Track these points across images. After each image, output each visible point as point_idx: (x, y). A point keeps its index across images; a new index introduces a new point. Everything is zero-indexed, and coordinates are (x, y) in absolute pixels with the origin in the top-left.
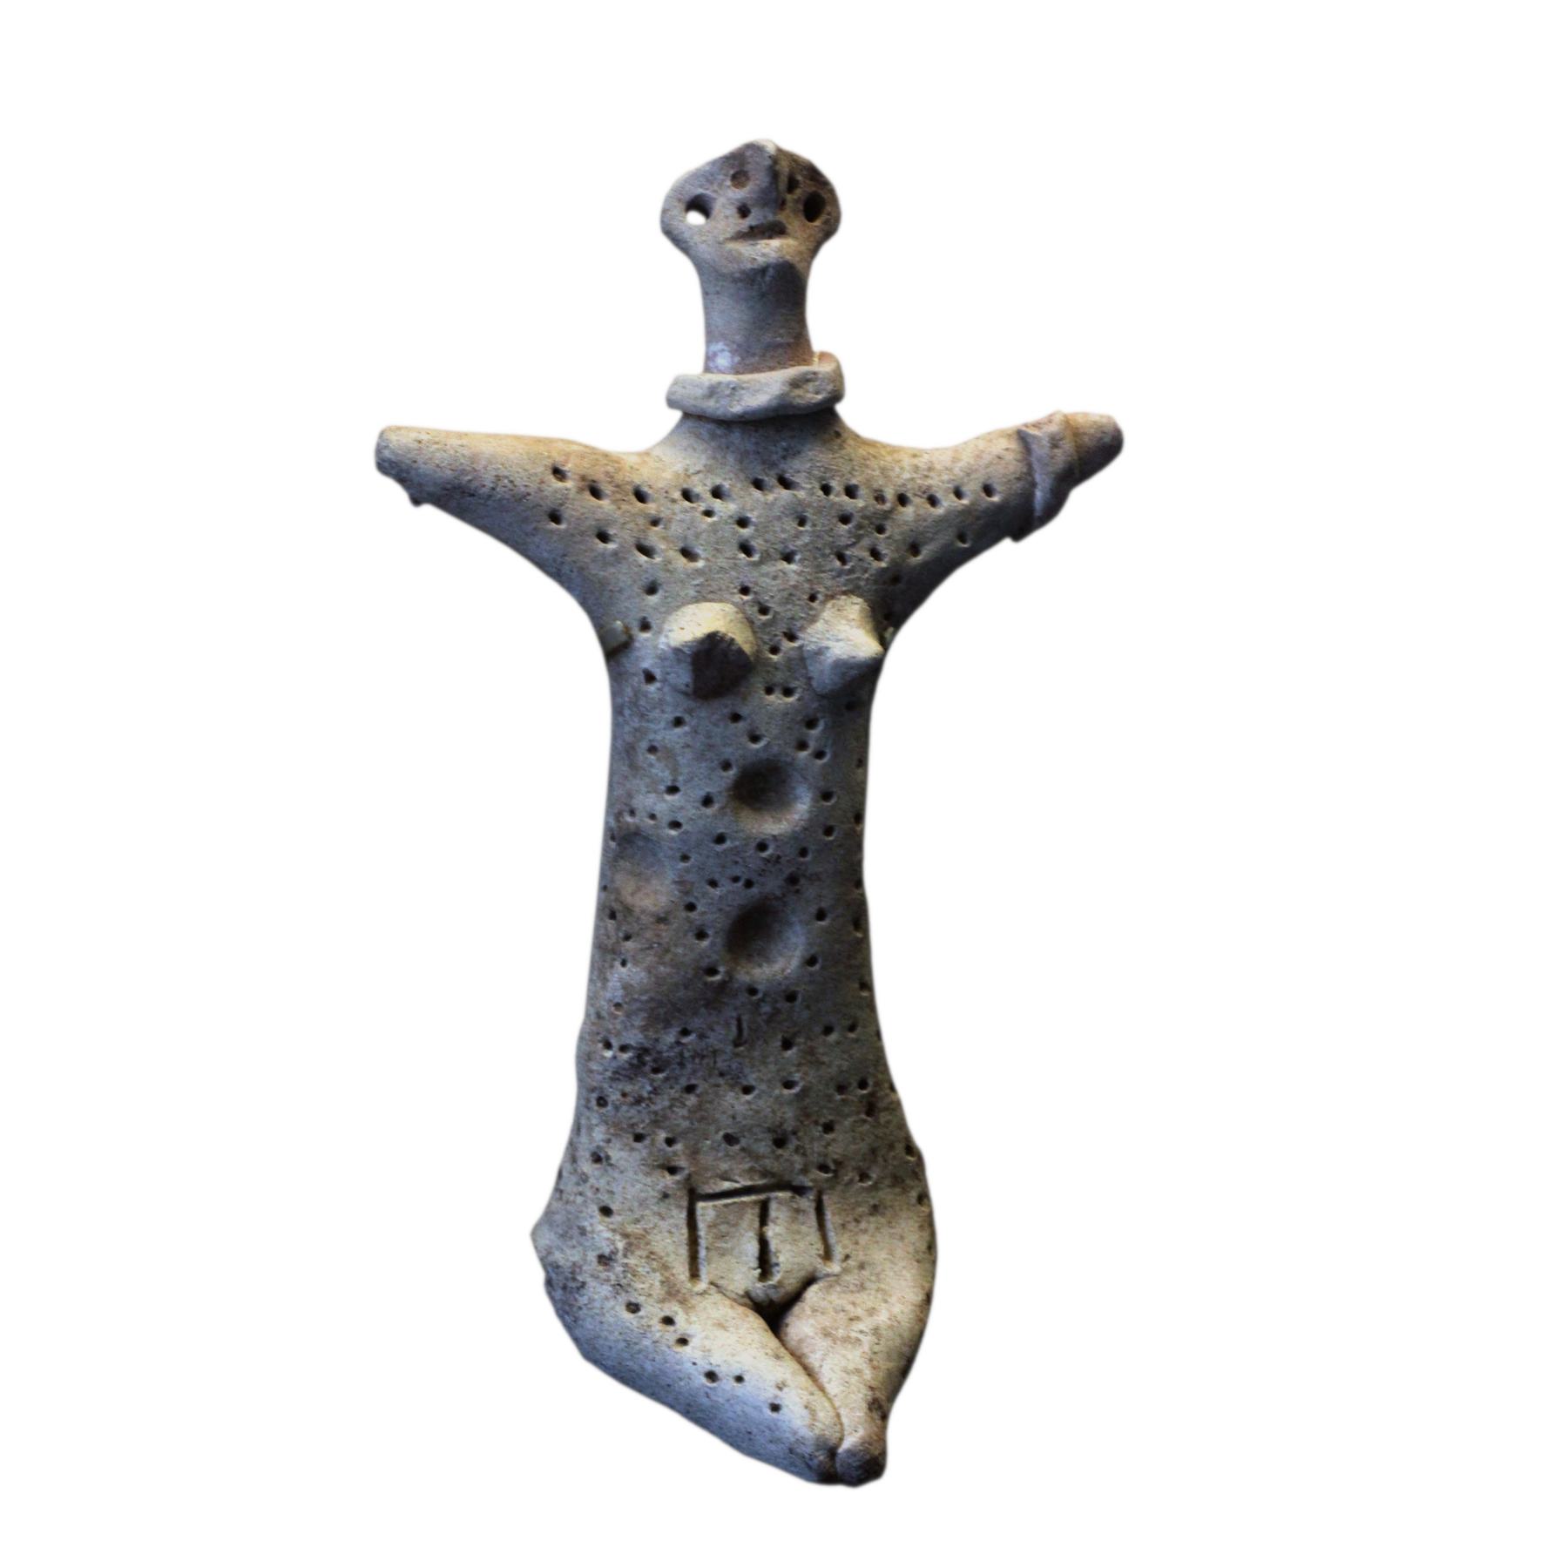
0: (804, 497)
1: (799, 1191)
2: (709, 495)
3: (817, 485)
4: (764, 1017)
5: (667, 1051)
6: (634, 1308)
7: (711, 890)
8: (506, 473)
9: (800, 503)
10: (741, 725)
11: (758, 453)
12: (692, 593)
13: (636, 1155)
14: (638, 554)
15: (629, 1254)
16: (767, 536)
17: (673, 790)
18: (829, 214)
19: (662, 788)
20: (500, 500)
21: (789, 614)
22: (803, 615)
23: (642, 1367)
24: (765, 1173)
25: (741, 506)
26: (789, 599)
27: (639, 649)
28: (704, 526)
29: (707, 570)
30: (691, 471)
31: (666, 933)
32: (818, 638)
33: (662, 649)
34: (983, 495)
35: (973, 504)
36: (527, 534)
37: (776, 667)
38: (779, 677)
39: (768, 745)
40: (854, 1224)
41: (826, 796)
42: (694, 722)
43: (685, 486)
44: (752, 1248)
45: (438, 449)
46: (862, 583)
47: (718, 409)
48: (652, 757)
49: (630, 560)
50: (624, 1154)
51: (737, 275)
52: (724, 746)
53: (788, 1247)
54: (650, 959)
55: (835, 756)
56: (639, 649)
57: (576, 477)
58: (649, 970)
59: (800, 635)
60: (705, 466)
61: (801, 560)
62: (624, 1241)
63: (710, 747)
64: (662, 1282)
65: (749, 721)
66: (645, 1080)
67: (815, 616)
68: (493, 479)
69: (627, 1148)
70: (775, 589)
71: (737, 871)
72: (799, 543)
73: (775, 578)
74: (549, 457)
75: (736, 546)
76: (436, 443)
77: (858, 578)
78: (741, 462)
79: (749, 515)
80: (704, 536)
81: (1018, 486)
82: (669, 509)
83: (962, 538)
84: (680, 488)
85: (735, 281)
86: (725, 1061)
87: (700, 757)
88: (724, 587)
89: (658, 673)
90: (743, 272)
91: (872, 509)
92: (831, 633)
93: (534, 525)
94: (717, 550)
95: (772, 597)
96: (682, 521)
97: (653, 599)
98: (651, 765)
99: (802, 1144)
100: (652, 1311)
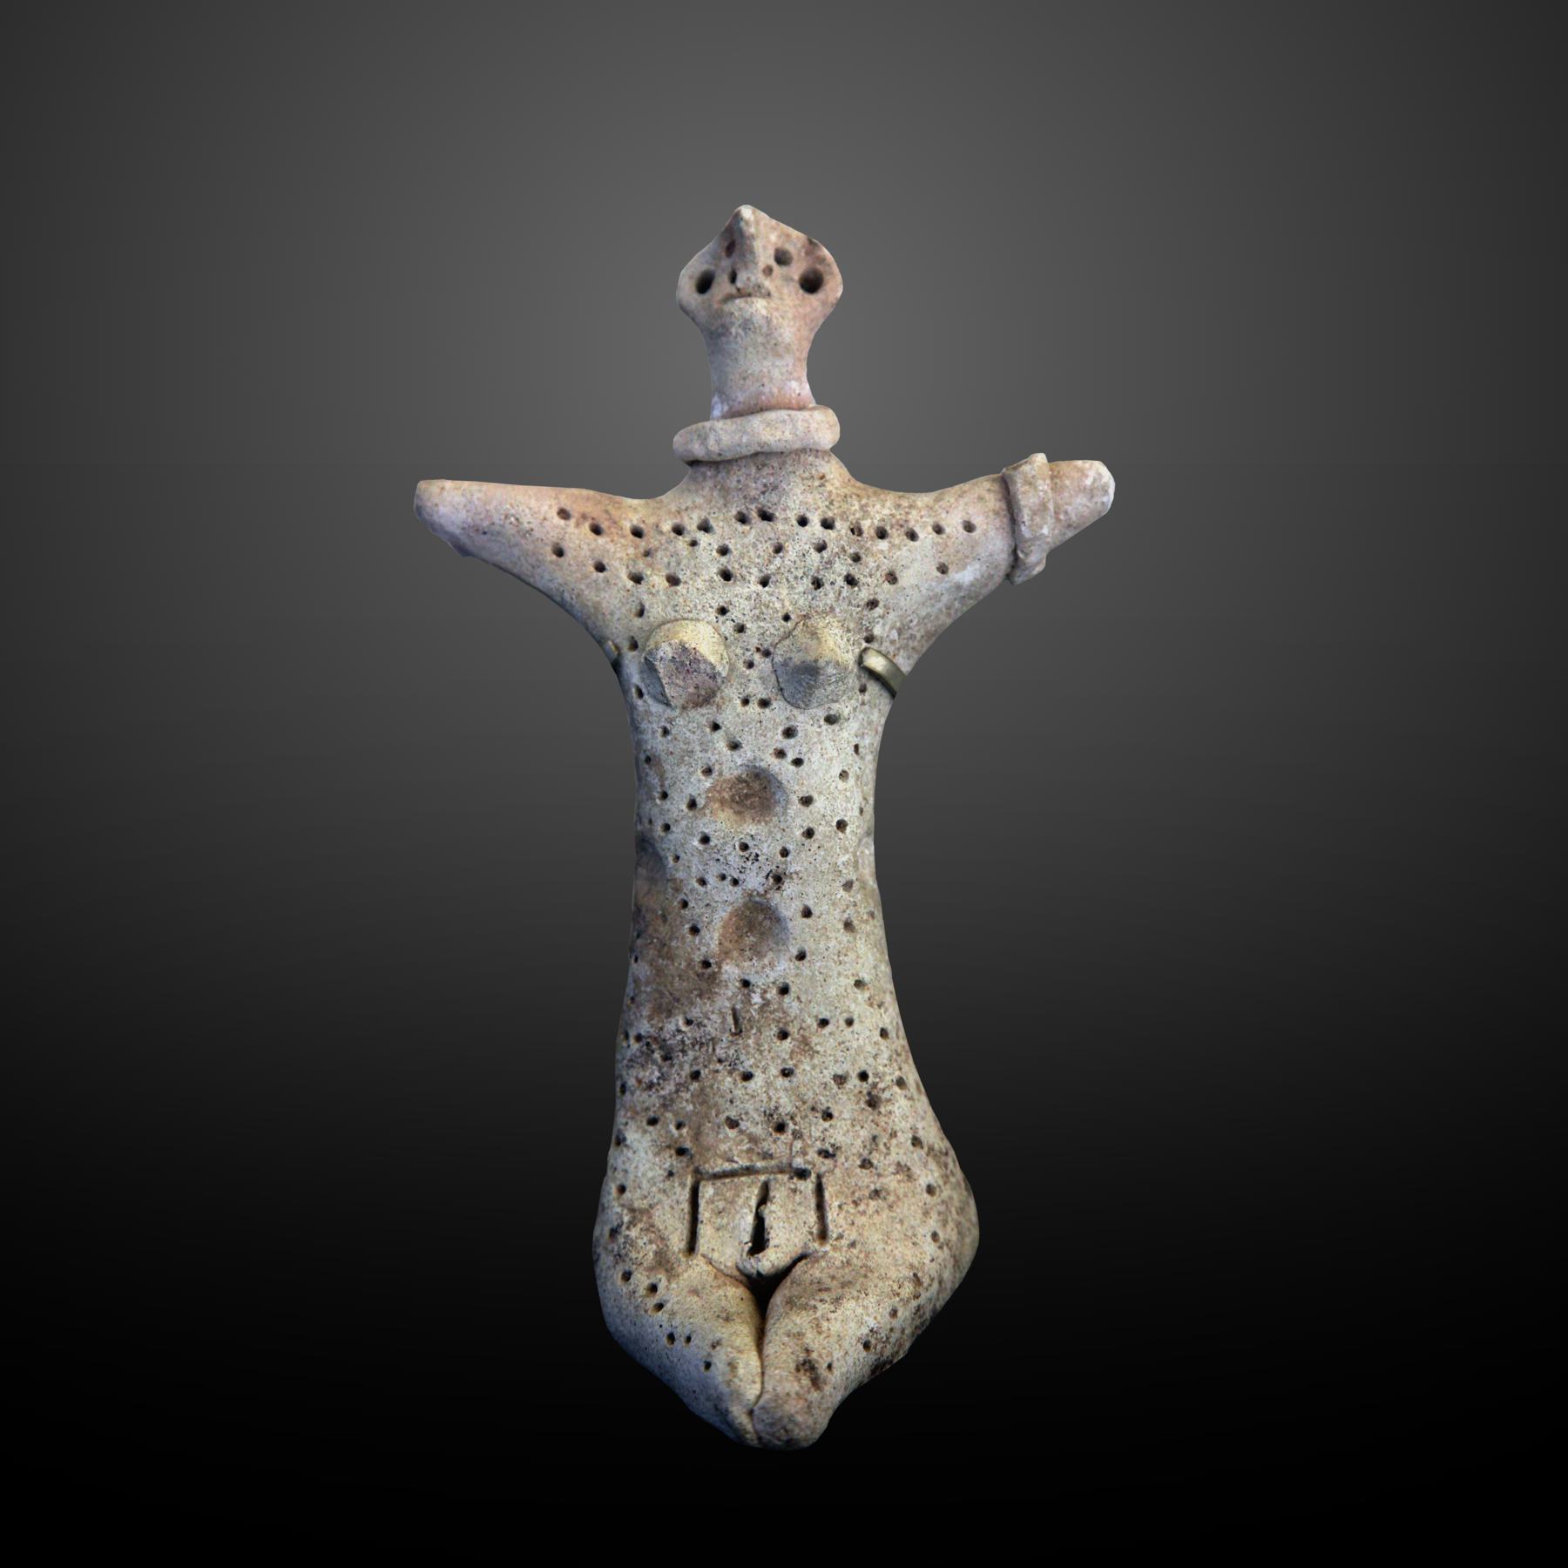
1: (802, 1174)
4: (756, 1007)
5: (670, 1039)
8: (513, 511)
13: (648, 1137)
15: (632, 1226)
23: (630, 1332)
40: (852, 1206)
50: (637, 1136)
62: (629, 1216)
64: (656, 1253)
66: (654, 1067)
69: (640, 1131)
86: (722, 1048)
99: (797, 1128)
100: (641, 1280)
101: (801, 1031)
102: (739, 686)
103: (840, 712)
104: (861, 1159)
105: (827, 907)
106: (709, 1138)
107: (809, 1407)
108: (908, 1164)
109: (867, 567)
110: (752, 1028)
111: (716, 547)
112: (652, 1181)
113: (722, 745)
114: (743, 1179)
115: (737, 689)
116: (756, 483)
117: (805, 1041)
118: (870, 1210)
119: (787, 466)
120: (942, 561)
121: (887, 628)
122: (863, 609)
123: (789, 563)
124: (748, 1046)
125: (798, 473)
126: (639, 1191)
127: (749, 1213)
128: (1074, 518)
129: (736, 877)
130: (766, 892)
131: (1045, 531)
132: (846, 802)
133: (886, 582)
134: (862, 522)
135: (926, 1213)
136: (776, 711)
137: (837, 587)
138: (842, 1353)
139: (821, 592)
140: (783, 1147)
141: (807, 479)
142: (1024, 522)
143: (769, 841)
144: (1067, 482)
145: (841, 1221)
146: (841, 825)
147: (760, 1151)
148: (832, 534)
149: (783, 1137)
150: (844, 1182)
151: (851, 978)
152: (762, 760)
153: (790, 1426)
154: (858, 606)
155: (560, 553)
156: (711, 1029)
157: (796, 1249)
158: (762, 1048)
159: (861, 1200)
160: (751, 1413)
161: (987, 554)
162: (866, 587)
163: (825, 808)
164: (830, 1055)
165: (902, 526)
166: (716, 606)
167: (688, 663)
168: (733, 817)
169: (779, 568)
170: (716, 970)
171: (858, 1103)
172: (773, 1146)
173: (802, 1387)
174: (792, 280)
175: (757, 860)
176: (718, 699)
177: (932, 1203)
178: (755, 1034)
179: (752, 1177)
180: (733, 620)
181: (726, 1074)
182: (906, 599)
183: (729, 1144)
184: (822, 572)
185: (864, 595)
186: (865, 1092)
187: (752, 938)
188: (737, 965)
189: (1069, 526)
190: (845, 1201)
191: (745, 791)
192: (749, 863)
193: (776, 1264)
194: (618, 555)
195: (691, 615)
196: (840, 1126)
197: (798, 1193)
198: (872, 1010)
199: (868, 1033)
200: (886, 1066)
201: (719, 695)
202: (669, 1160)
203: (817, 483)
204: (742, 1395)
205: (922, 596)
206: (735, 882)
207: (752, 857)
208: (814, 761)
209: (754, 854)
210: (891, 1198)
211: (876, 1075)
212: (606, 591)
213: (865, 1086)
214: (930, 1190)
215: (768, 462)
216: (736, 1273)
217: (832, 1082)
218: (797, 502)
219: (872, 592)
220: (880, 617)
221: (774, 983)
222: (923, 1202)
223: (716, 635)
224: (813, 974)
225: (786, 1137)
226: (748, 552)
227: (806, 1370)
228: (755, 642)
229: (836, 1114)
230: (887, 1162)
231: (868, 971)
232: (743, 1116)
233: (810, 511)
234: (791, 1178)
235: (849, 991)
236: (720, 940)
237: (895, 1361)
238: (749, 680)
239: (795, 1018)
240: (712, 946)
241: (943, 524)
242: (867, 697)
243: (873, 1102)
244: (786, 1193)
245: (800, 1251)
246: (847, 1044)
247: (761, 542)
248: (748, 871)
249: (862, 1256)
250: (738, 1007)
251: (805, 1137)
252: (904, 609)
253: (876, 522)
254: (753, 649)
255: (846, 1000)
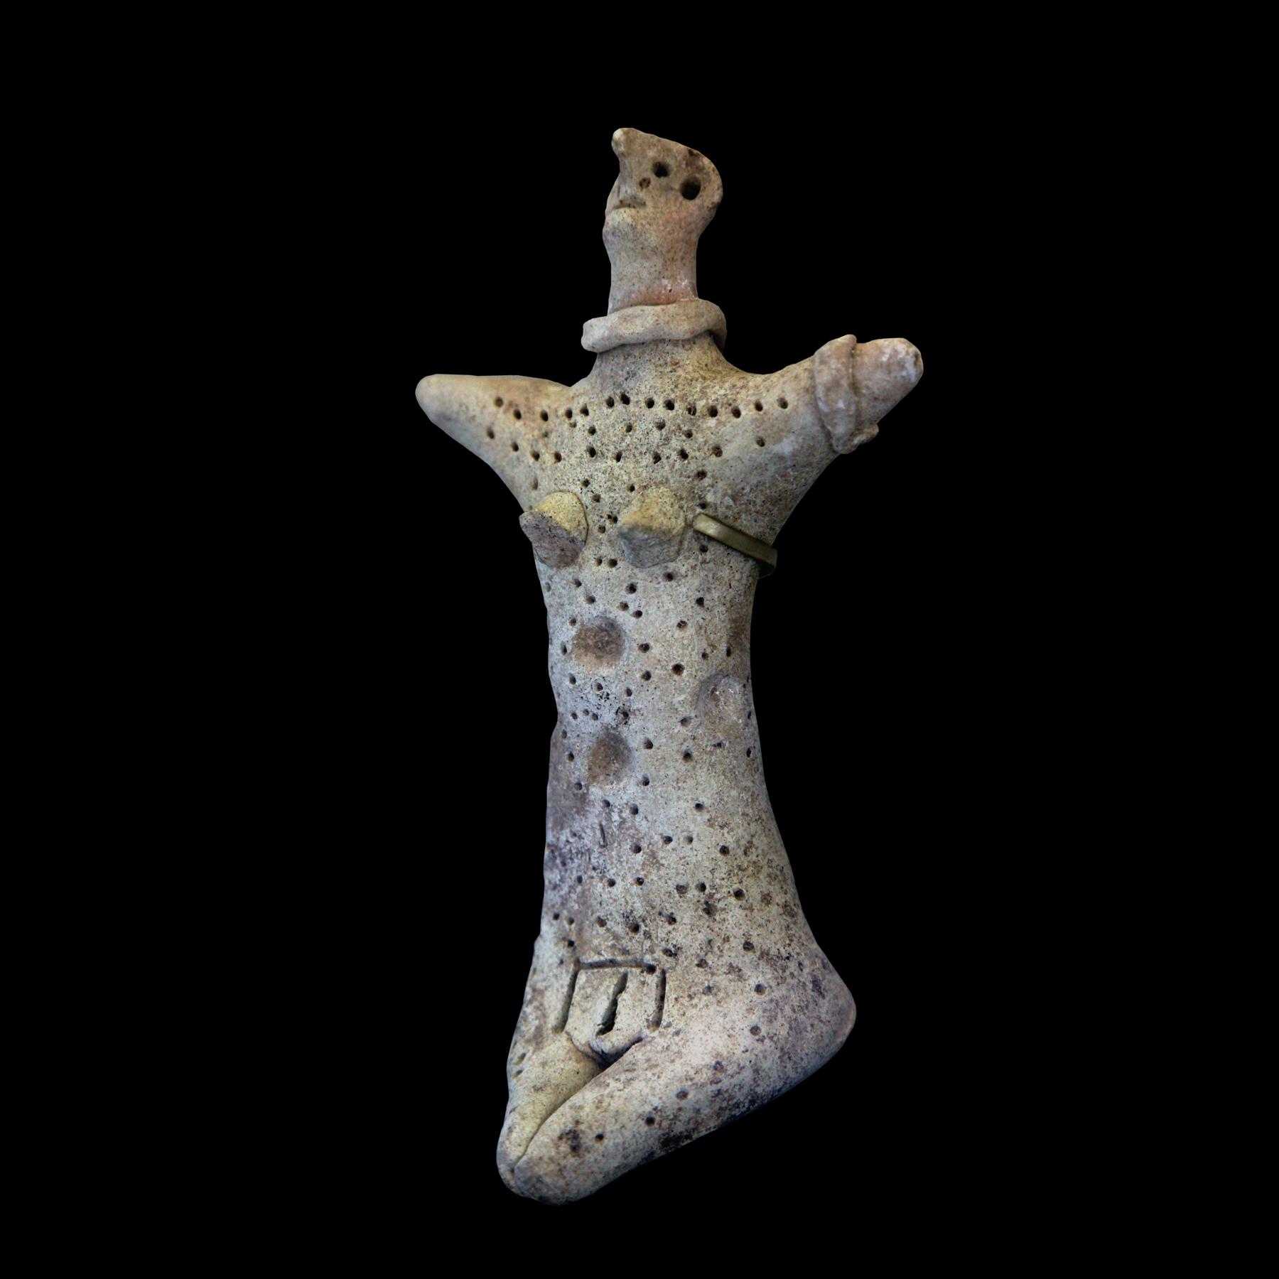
1: (651, 969)
4: (616, 824)
40: (687, 999)
44: (602, 1006)
53: (628, 1011)
99: (647, 929)
101: (650, 846)
102: (594, 549)
103: (677, 570)
104: (699, 959)
105: (664, 740)
106: (587, 934)
107: (560, 1170)
108: (740, 965)
109: (696, 442)
110: (614, 842)
111: (588, 428)
112: (550, 966)
113: (582, 599)
114: (607, 970)
115: (593, 551)
116: (622, 371)
117: (653, 855)
118: (701, 1005)
119: (646, 355)
120: (760, 434)
121: (719, 495)
122: (693, 480)
123: (636, 440)
124: (612, 857)
125: (653, 361)
126: (541, 974)
127: (606, 999)
128: (877, 392)
129: (595, 712)
130: (617, 725)
131: (841, 405)
132: (683, 649)
133: (714, 456)
134: (697, 403)
135: (750, 1010)
136: (621, 569)
137: (671, 461)
138: (617, 1126)
139: (658, 465)
140: (636, 945)
141: (661, 365)
142: (820, 398)
143: (616, 683)
144: (866, 360)
145: (675, 1012)
146: (678, 669)
147: (620, 947)
148: (672, 413)
149: (637, 937)
150: (683, 978)
151: (690, 802)
152: (611, 612)
153: (538, 1185)
154: (689, 477)
155: (491, 435)
156: (587, 841)
157: (634, 1033)
158: (622, 860)
159: (695, 995)
160: (512, 1171)
161: (799, 427)
162: (695, 460)
163: (661, 654)
164: (673, 868)
165: (730, 405)
166: (582, 478)
167: (548, 529)
168: (594, 660)
169: (628, 445)
170: (585, 791)
171: (696, 910)
172: (630, 944)
173: (558, 1153)
174: (672, 189)
175: (608, 699)
176: (580, 560)
177: (759, 1001)
178: (617, 847)
179: (614, 969)
180: (592, 491)
181: (598, 880)
182: (731, 470)
183: (599, 940)
184: (661, 448)
185: (693, 467)
186: (703, 901)
187: (617, 765)
188: (601, 788)
189: (876, 399)
190: (681, 994)
191: (606, 639)
192: (603, 701)
193: (616, 1044)
194: (527, 437)
195: (565, 488)
196: (681, 930)
197: (646, 985)
198: (712, 830)
199: (706, 850)
200: (723, 879)
201: (580, 555)
202: (563, 951)
203: (669, 369)
204: (507, 1155)
205: (745, 466)
206: (595, 717)
207: (604, 696)
208: (651, 612)
209: (605, 694)
210: (721, 995)
211: (713, 887)
213: (703, 897)
214: (759, 989)
215: (632, 352)
216: (588, 1050)
217: (675, 891)
218: (648, 387)
219: (700, 464)
220: (709, 486)
221: (627, 804)
222: (750, 999)
223: (578, 505)
224: (656, 797)
225: (639, 936)
226: (608, 431)
227: (568, 1139)
228: (607, 510)
229: (678, 919)
230: (720, 963)
231: (709, 796)
232: (609, 917)
233: (657, 394)
234: (642, 972)
235: (688, 812)
236: (589, 766)
237: (695, 1136)
238: (602, 543)
239: (645, 835)
240: (583, 771)
241: (763, 402)
242: (708, 556)
243: (709, 910)
244: (637, 985)
245: (637, 1036)
246: (687, 859)
247: (618, 424)
248: (603, 708)
249: (680, 1043)
250: (604, 823)
251: (653, 937)
252: (732, 478)
253: (710, 401)
254: (606, 516)
255: (685, 820)
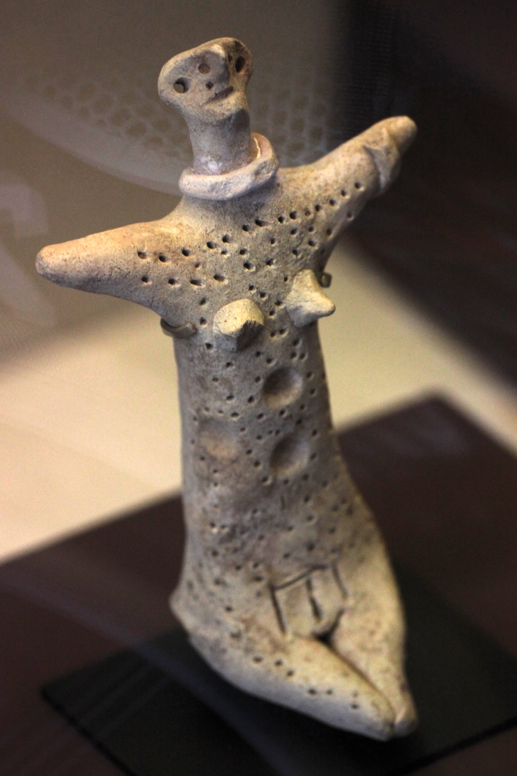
0: (271, 229)
2: (222, 242)
3: (277, 220)
6: (258, 660)
7: (258, 441)
8: (115, 265)
9: (270, 232)
10: (262, 357)
11: (242, 212)
12: (225, 298)
14: (192, 285)
16: (257, 256)
17: (230, 397)
18: (248, 65)
19: (224, 398)
20: (115, 279)
21: (276, 293)
22: (283, 291)
24: (307, 566)
25: (240, 243)
26: (275, 285)
27: (202, 334)
28: (224, 261)
29: (230, 284)
30: (208, 231)
31: (239, 468)
32: (295, 302)
33: (216, 333)
34: (356, 189)
35: (352, 197)
36: (132, 292)
37: (274, 322)
38: (277, 326)
39: (277, 363)
41: (309, 375)
42: (238, 363)
43: (208, 241)
44: (308, 608)
45: (76, 262)
46: (308, 262)
47: (218, 196)
48: (216, 384)
49: (189, 290)
51: (215, 123)
52: (255, 370)
54: (231, 482)
55: (310, 354)
56: (202, 334)
57: (151, 254)
58: (232, 487)
59: (284, 301)
60: (215, 226)
61: (276, 263)
63: (249, 373)
65: (266, 354)
67: (288, 289)
68: (108, 270)
70: (266, 283)
71: (271, 428)
72: (274, 254)
73: (265, 276)
74: (134, 247)
75: (242, 266)
76: (74, 258)
77: (306, 260)
78: (234, 219)
79: (246, 248)
80: (225, 266)
81: (371, 178)
82: (202, 256)
83: (349, 215)
84: (205, 243)
85: (214, 126)
87: (244, 379)
88: (241, 291)
89: (214, 344)
90: (218, 121)
91: (305, 221)
92: (300, 297)
93: (134, 287)
94: (233, 272)
95: (266, 287)
96: (211, 261)
97: (205, 307)
98: (217, 387)
100: (269, 661)
212: (181, 296)
